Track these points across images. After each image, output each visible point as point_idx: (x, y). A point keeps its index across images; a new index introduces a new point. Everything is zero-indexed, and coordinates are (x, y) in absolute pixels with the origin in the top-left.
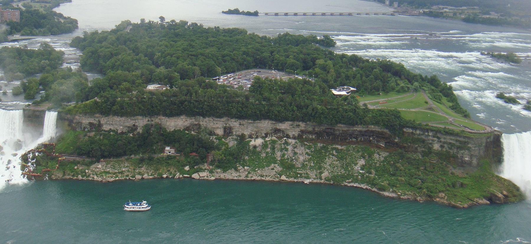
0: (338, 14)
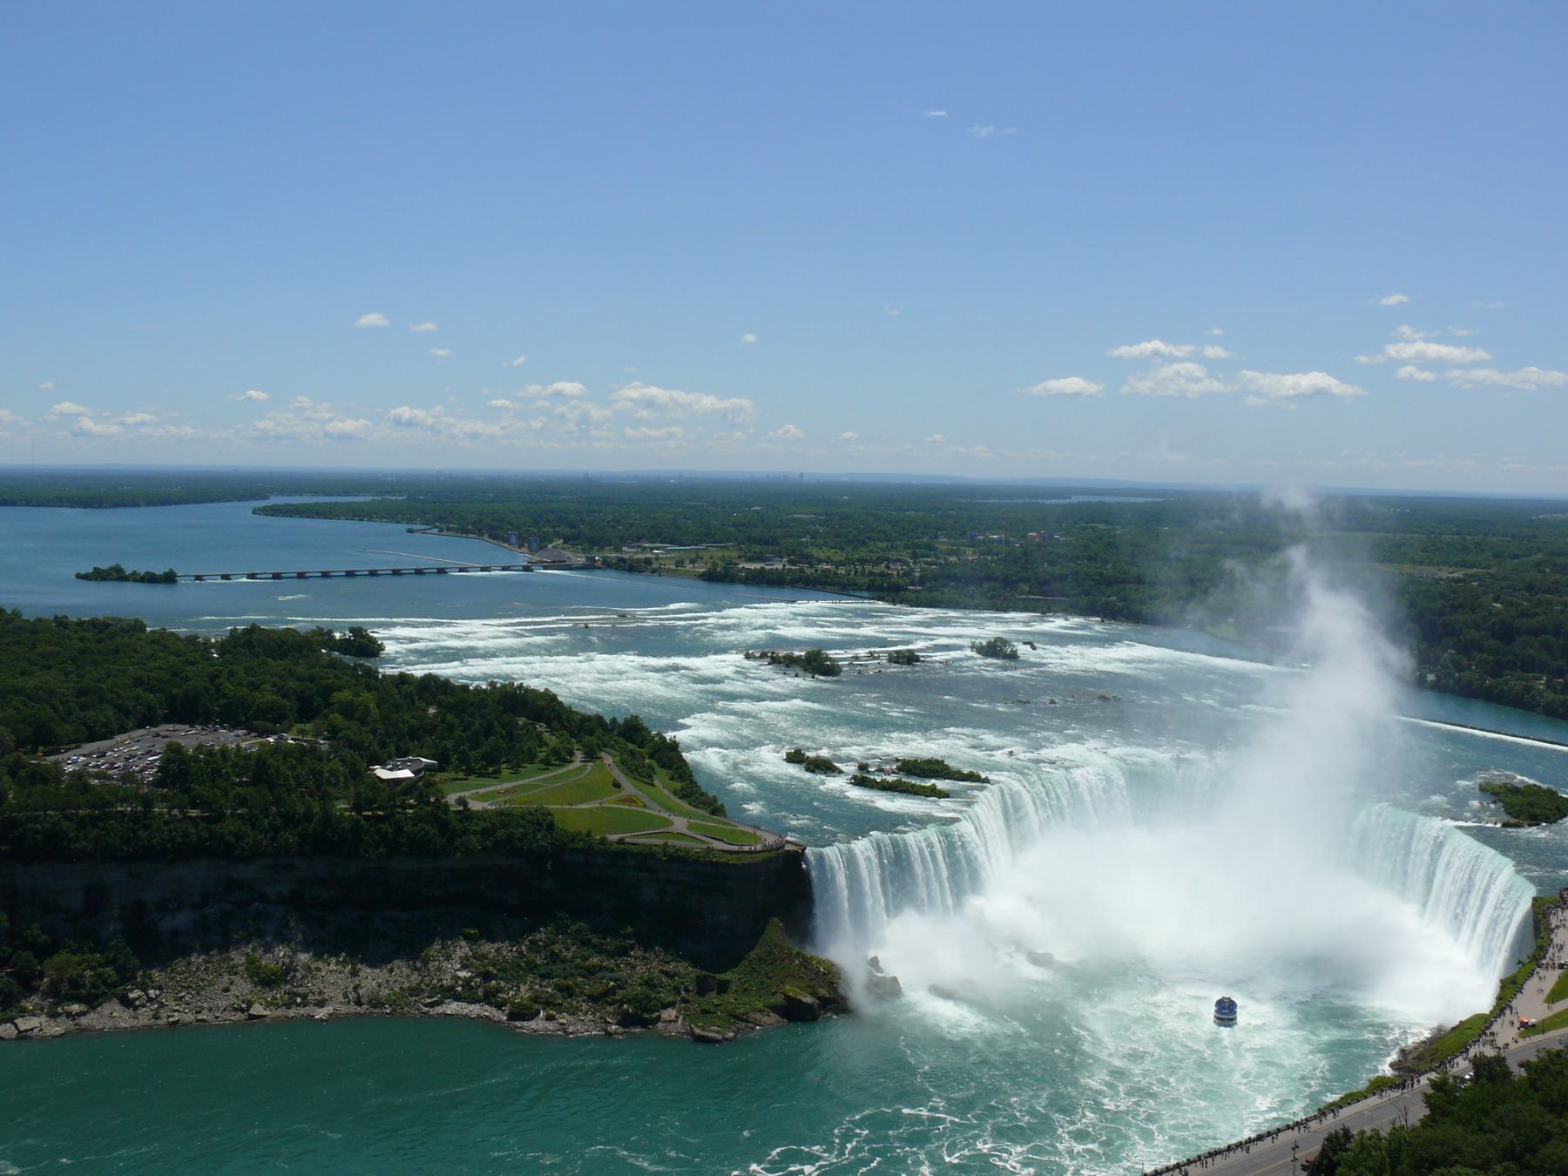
0: (431, 571)
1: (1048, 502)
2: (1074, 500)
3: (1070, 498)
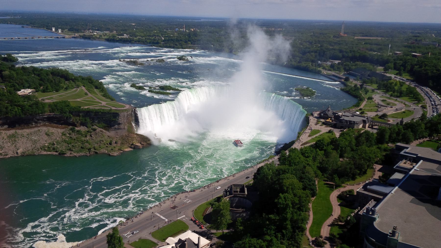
2: (202, 20)
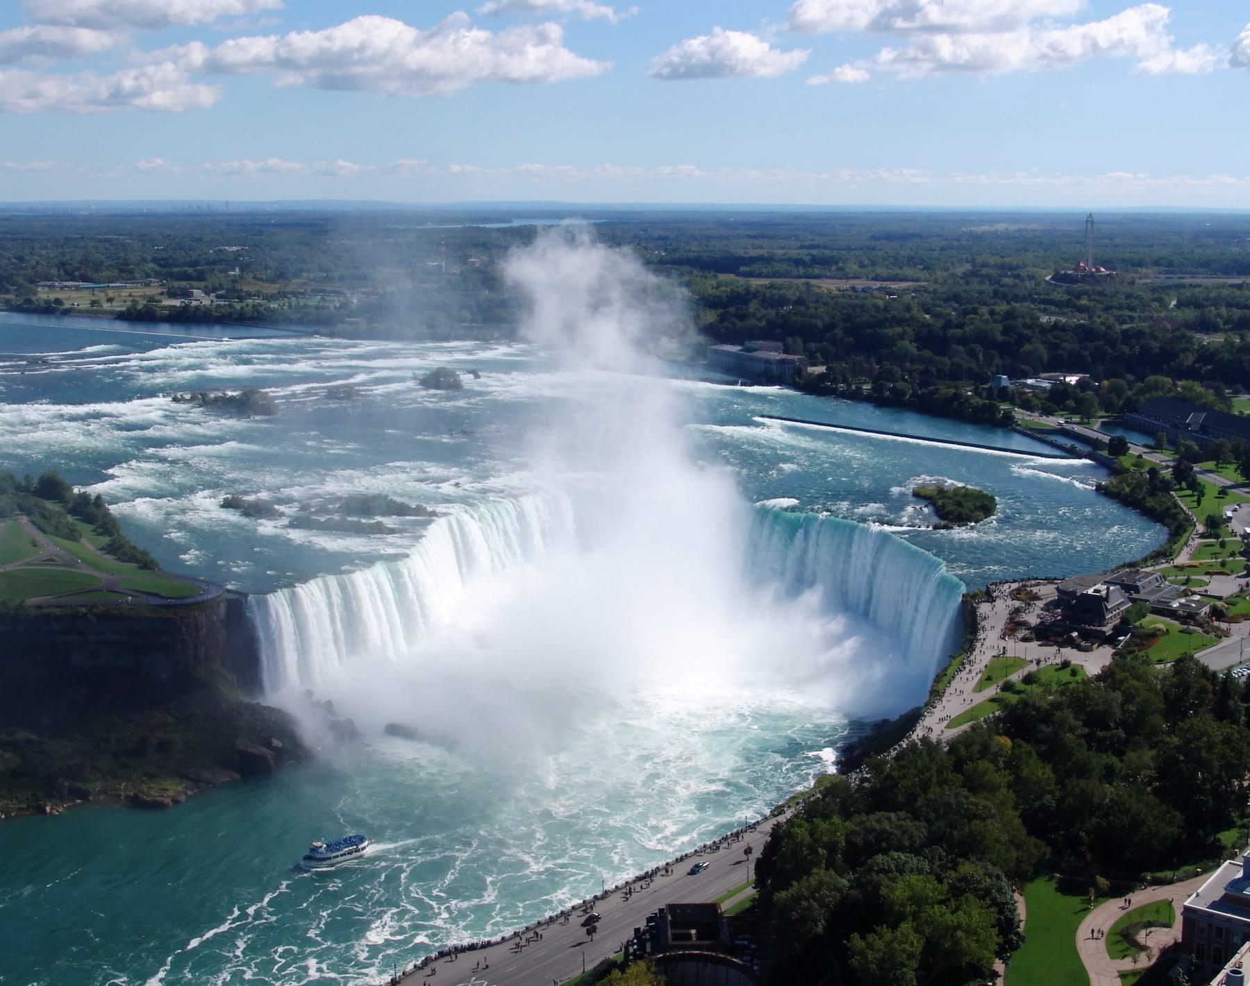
1: (487, 226)
3: (512, 222)
